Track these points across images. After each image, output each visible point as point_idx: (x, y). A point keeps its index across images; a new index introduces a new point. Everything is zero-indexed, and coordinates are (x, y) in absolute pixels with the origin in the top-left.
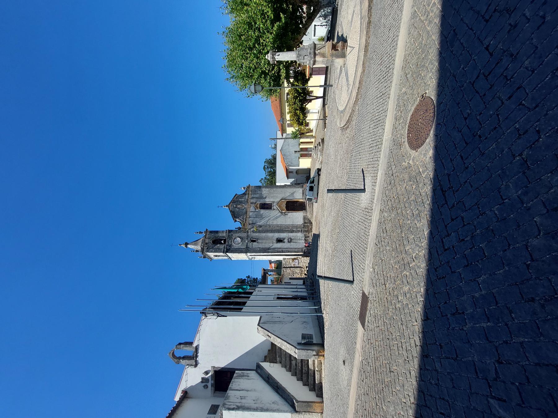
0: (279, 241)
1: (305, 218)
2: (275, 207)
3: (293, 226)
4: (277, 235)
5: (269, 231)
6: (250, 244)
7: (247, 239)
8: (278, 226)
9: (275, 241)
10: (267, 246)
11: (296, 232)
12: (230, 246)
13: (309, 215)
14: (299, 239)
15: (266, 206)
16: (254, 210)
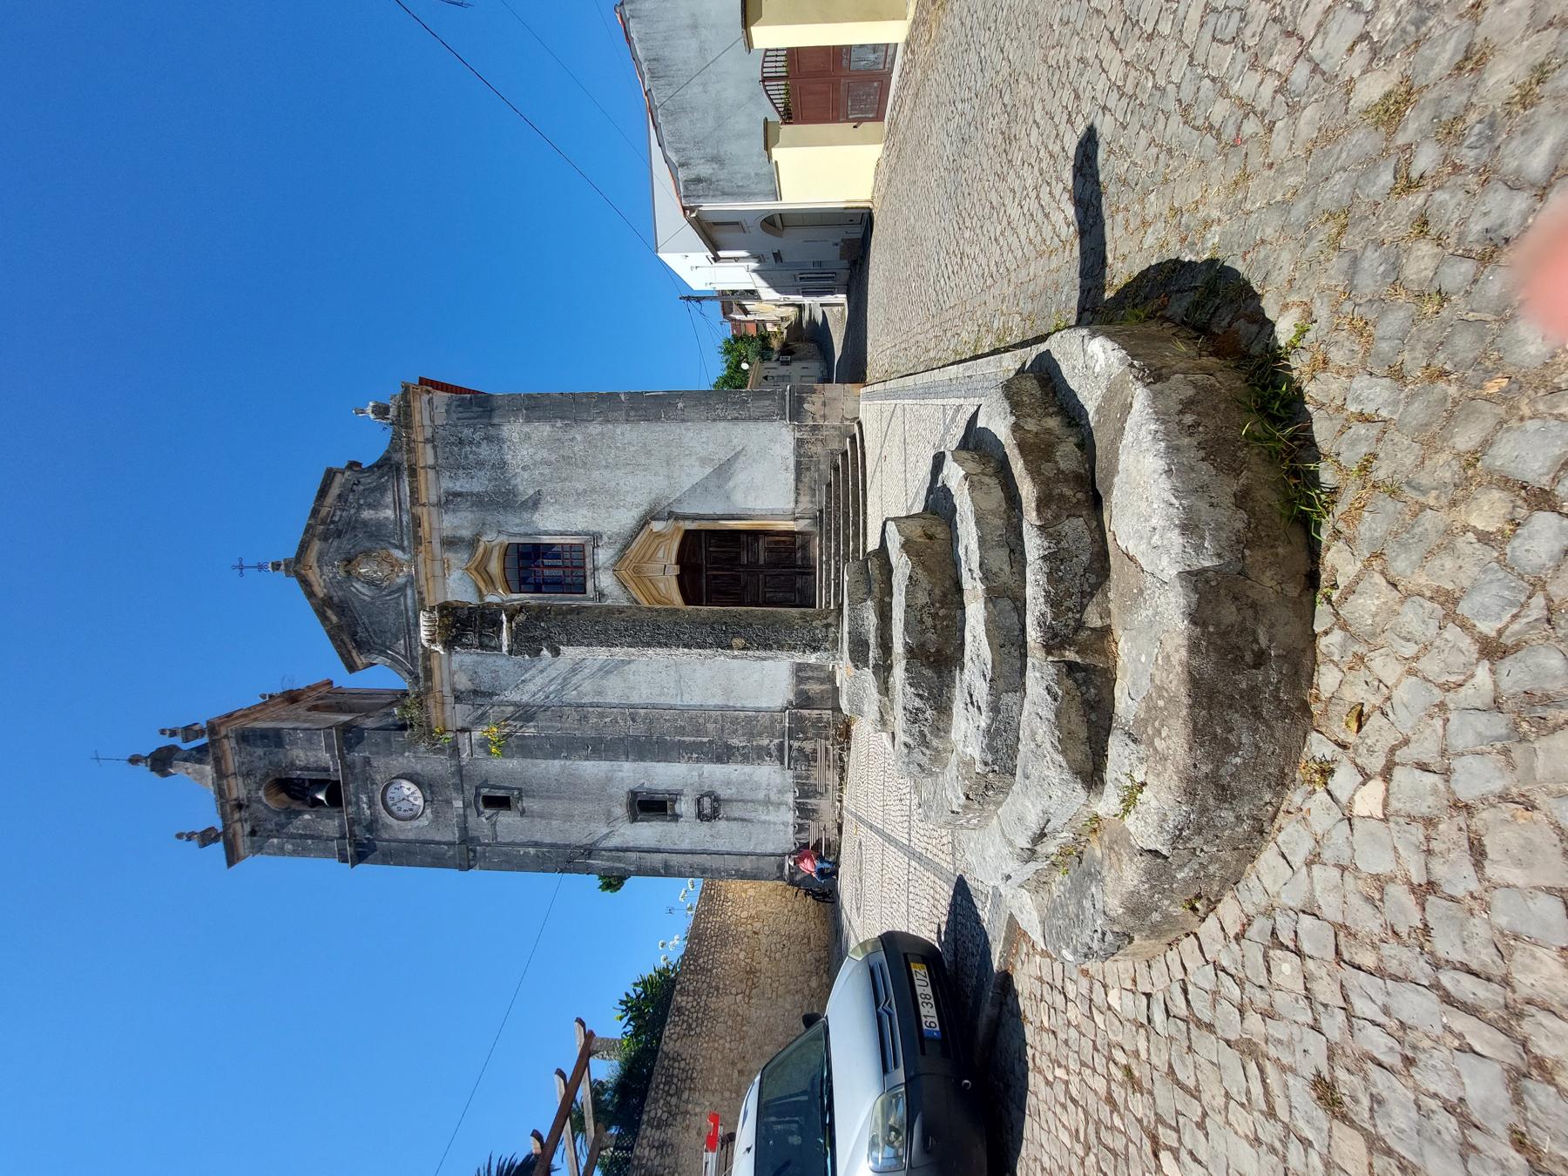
0: (650, 806)
4: (632, 774)
6: (481, 823)
7: (460, 789)
8: (632, 711)
9: (620, 811)
10: (578, 834)
11: (746, 759)
12: (372, 825)
14: (767, 802)
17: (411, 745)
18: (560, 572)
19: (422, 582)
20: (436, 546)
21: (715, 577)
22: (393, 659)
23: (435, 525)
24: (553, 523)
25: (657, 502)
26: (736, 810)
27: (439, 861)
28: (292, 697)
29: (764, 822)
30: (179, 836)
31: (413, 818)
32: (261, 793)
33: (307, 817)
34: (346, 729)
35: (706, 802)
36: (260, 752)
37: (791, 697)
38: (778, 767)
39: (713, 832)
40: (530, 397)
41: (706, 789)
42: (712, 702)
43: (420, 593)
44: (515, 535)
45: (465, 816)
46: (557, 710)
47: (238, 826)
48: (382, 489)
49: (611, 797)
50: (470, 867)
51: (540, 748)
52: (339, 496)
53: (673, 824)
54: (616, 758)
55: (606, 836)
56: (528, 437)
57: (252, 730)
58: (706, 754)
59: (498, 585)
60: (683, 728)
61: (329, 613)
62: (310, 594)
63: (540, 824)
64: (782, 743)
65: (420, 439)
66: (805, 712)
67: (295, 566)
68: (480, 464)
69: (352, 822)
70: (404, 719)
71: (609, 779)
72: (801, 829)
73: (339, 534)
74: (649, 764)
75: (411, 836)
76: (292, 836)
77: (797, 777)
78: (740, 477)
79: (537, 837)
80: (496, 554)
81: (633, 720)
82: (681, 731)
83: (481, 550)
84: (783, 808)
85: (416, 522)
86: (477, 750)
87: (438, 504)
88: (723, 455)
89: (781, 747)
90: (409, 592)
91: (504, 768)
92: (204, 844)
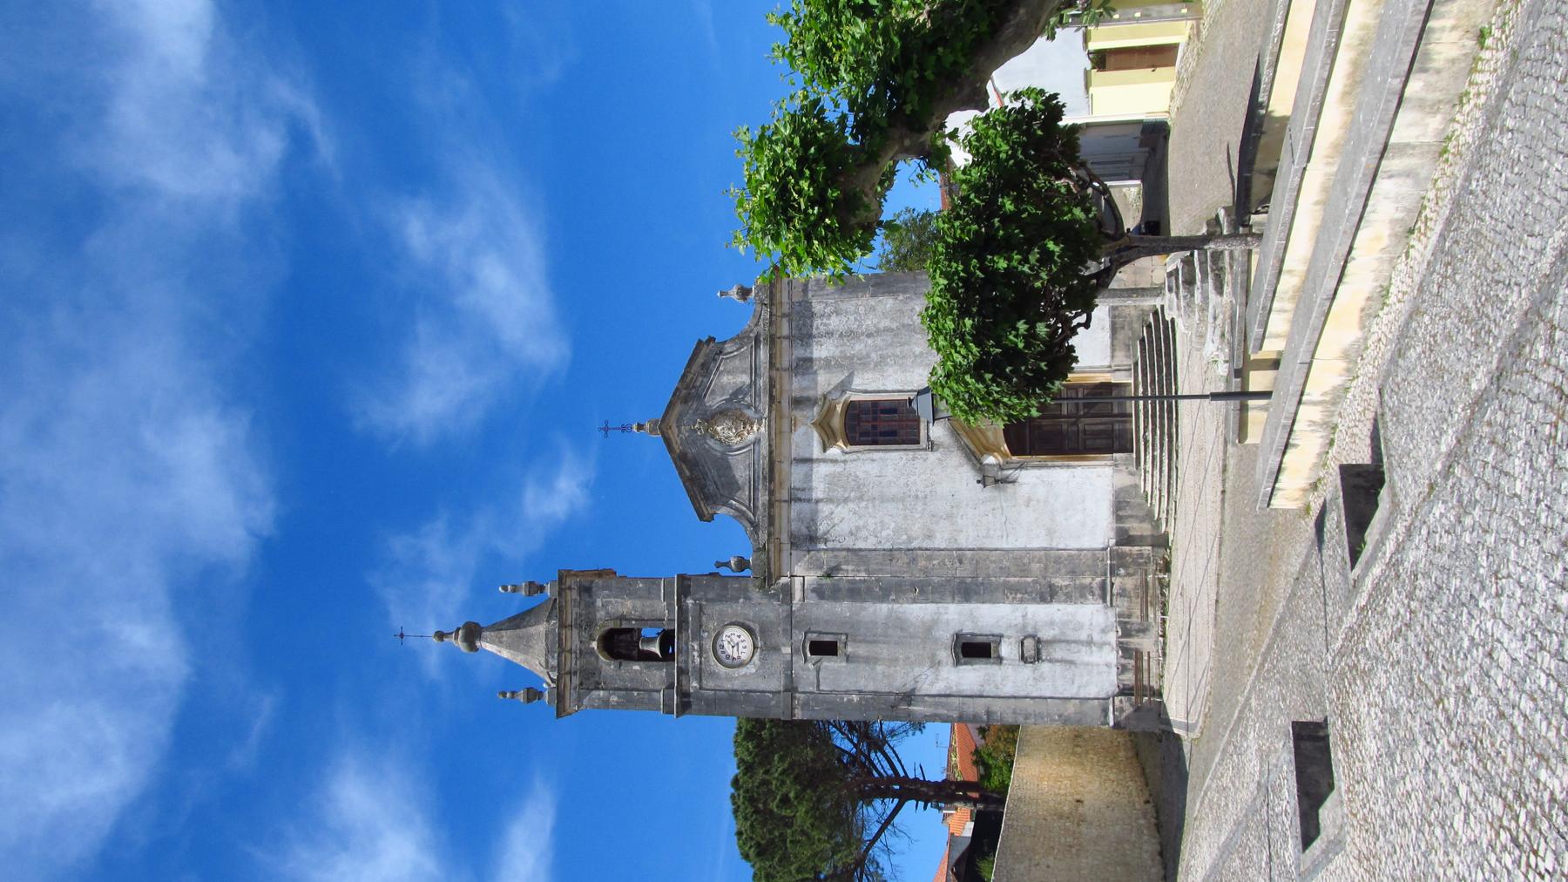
0: (974, 649)
1: (1121, 504)
3: (1054, 559)
5: (913, 586)
8: (959, 554)
9: (945, 655)
11: (1069, 598)
20: (785, 404)
26: (1059, 652)
31: (742, 665)
32: (594, 645)
33: (636, 667)
35: (1029, 643)
37: (1112, 534)
38: (1100, 606)
41: (1030, 630)
42: (1035, 544)
49: (936, 641)
52: (703, 365)
53: (996, 667)
56: (873, 309)
63: (863, 669)
64: (1104, 583)
66: (1126, 549)
69: (681, 672)
72: (1123, 669)
75: (737, 685)
77: (1120, 615)
80: (839, 408)
82: (1004, 571)
84: (1106, 649)
86: (809, 594)
89: (1103, 586)
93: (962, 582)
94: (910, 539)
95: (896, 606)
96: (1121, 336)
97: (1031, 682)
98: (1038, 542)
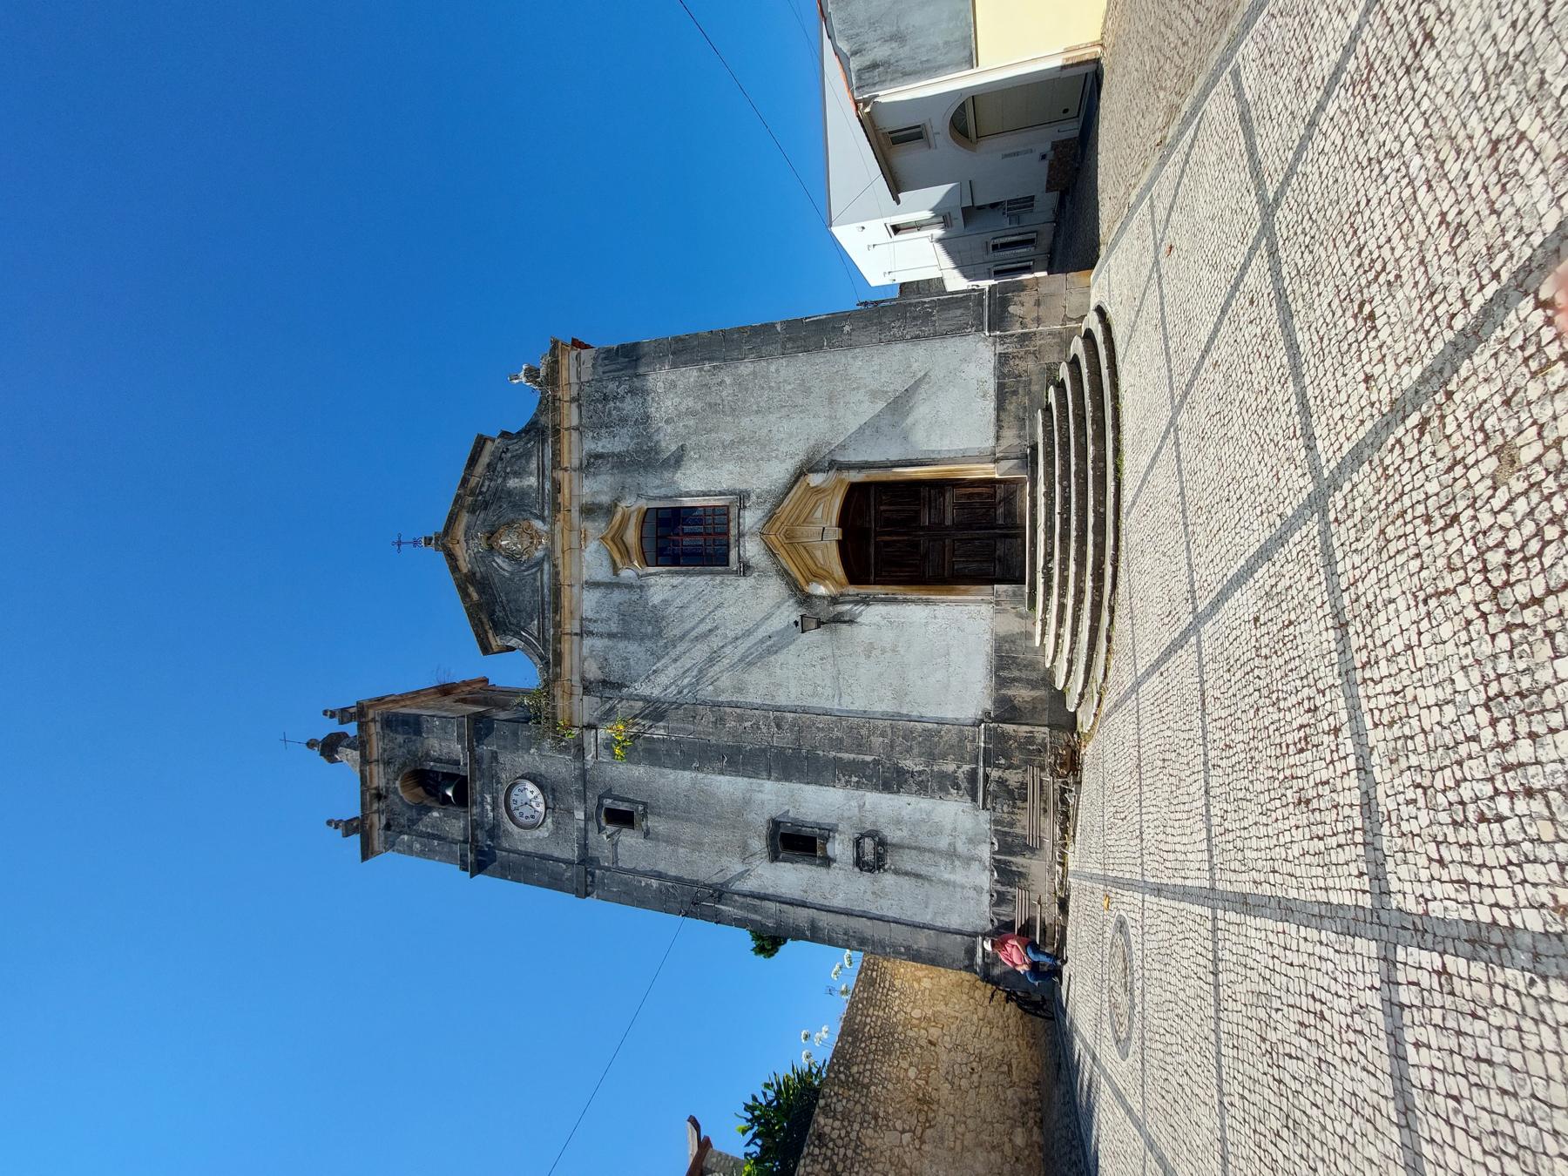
0: (796, 842)
1: (1008, 661)
2: (752, 549)
6: (602, 840)
8: (777, 715)
9: (759, 844)
10: (707, 867)
11: (923, 789)
12: (494, 831)
13: (1053, 645)
14: (952, 854)
15: (688, 538)
16: (603, 573)
17: (535, 741)
18: (700, 541)
19: (558, 553)
20: (575, 514)
21: (887, 544)
22: (527, 642)
23: (576, 492)
24: (697, 484)
25: (815, 449)
26: (908, 861)
27: (555, 883)
28: (445, 690)
29: (947, 883)
30: (329, 823)
31: (534, 826)
32: (398, 784)
33: (435, 814)
34: (476, 719)
35: (868, 844)
36: (400, 739)
37: (989, 705)
38: (967, 804)
39: (876, 887)
40: (677, 340)
41: (869, 827)
42: (879, 708)
43: (555, 566)
44: (654, 498)
45: (586, 830)
46: (690, 708)
47: (375, 817)
48: (527, 455)
49: (747, 825)
50: (587, 894)
51: (669, 754)
53: (823, 871)
54: (755, 775)
55: (741, 876)
56: (673, 385)
57: (396, 714)
58: (869, 778)
59: (634, 557)
60: (841, 740)
61: (471, 589)
62: (455, 568)
63: (665, 850)
64: (974, 772)
65: (567, 398)
66: (1009, 728)
67: (443, 541)
68: (623, 421)
69: (476, 825)
70: (536, 717)
71: (747, 802)
72: (1000, 899)
73: (486, 506)
74: (796, 786)
75: (530, 848)
76: (421, 835)
78: (922, 411)
79: (661, 867)
80: (633, 521)
81: (778, 726)
82: (838, 744)
83: (618, 517)
84: (975, 866)
85: (557, 487)
86: (603, 752)
87: (580, 468)
88: (899, 385)
90: (546, 566)
91: (630, 775)
92: (346, 835)
93: (781, 751)
94: (718, 691)
95: (701, 776)
96: (1012, 407)
97: (869, 896)
98: (884, 705)
